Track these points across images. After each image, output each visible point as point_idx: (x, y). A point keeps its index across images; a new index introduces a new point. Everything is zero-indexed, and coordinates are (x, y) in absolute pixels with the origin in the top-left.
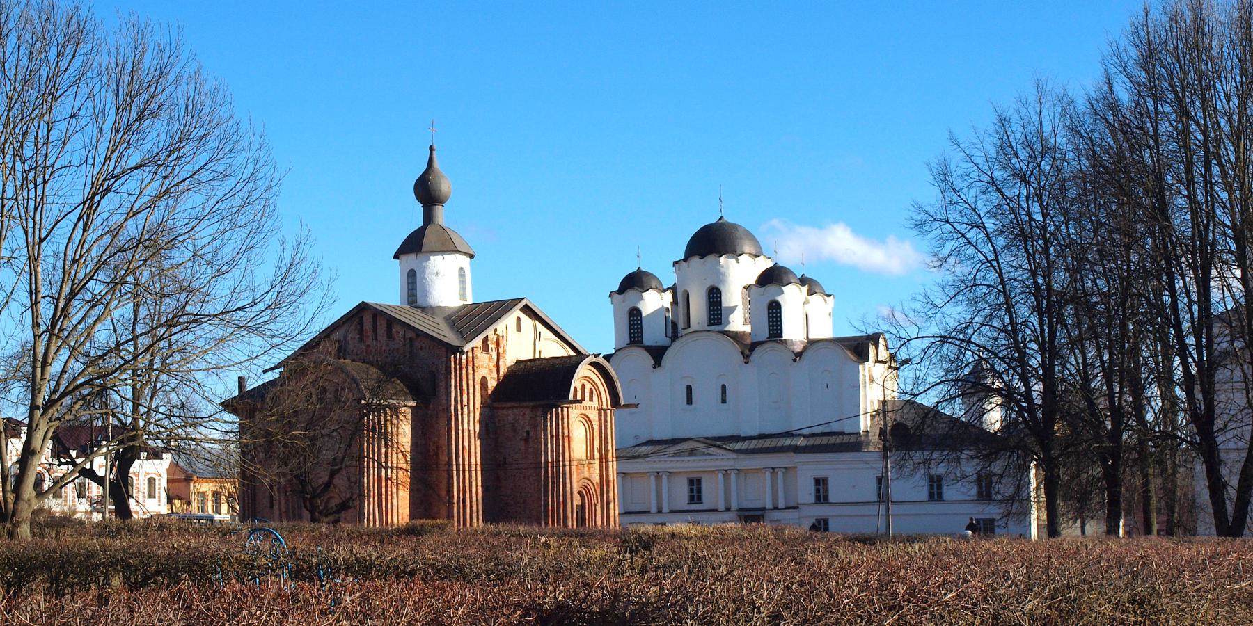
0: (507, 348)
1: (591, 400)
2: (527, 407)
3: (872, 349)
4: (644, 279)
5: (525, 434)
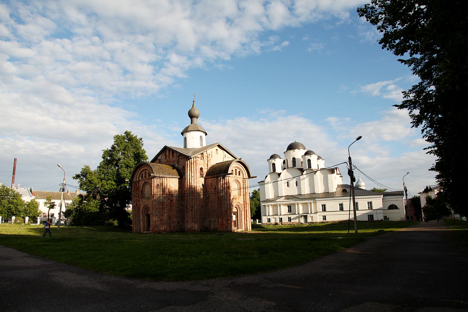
0: (212, 159)
1: (239, 174)
2: (215, 177)
3: (335, 170)
4: (276, 156)
5: (215, 187)
